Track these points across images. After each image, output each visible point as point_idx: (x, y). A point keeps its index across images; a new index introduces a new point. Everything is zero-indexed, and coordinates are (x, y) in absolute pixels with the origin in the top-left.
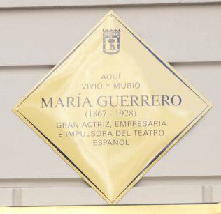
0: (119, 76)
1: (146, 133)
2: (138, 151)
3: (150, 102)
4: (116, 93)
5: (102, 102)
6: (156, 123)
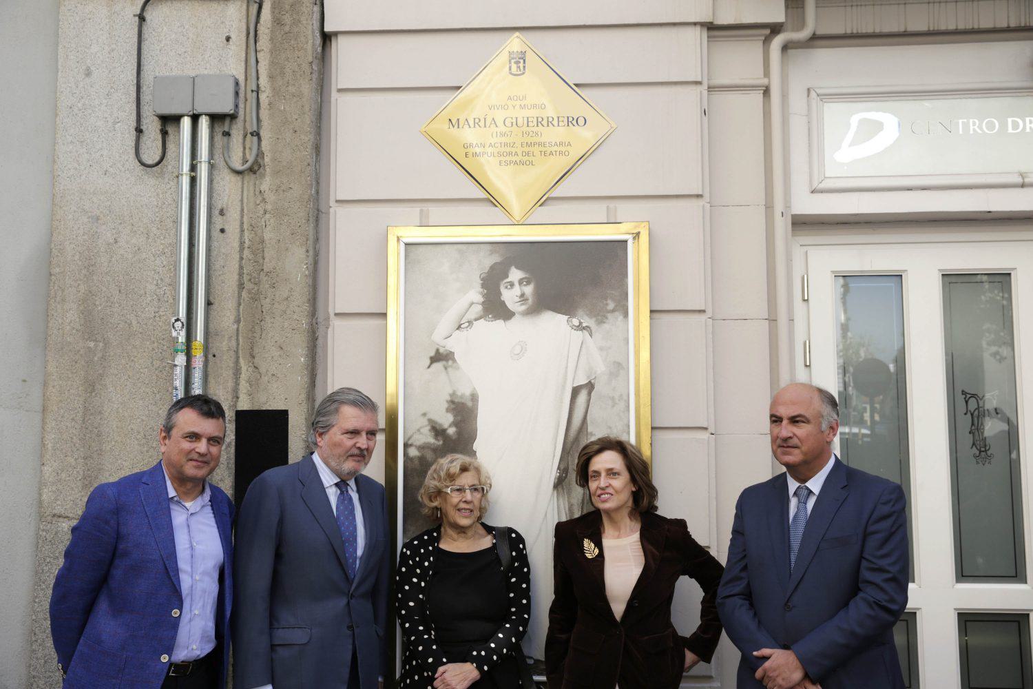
0: (525, 97)
1: (551, 153)
2: (544, 172)
3: (555, 122)
4: (522, 114)
5: (508, 122)
6: (561, 144)
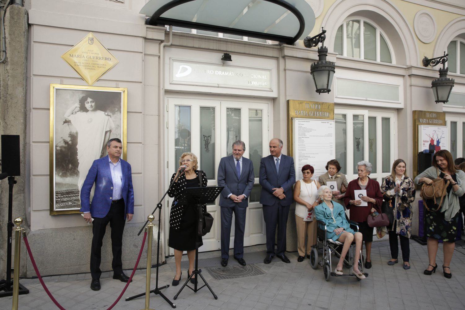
0: (93, 51)
1: (100, 67)
2: (97, 73)
3: (102, 59)
4: (92, 55)
5: (88, 57)
6: (103, 65)
